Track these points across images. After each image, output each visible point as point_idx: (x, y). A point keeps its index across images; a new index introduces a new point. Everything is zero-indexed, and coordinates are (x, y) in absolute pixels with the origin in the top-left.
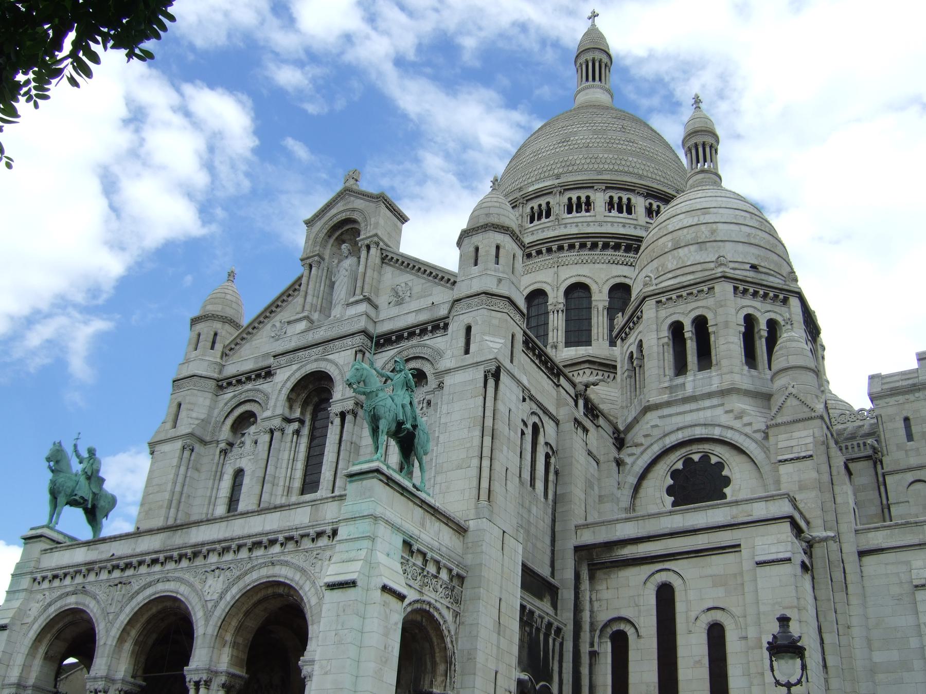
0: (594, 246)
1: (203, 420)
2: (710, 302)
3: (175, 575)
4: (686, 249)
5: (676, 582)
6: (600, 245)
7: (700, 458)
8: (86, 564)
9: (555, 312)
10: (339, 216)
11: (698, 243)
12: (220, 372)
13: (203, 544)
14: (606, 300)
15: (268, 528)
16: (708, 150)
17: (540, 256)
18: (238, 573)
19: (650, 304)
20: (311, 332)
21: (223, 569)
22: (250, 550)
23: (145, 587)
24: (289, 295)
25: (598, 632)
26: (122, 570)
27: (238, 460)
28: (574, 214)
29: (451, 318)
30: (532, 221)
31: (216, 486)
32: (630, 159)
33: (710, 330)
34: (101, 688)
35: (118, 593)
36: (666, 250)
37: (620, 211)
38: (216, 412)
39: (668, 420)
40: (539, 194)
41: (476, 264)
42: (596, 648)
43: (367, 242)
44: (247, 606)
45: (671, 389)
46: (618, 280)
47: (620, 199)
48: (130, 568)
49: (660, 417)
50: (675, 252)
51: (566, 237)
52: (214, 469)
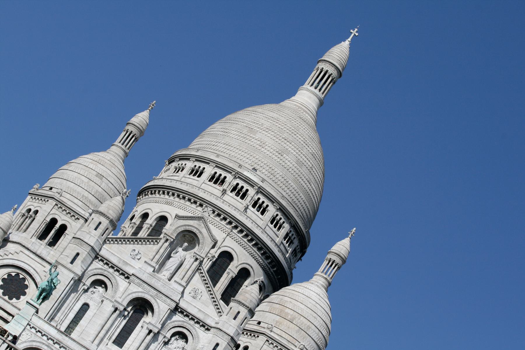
9: (209, 260)
12: (100, 250)
14: (235, 274)
17: (223, 221)
20: (154, 279)
27: (89, 300)
28: (254, 210)
29: (212, 330)
32: (301, 195)
36: (287, 318)
40: (247, 180)
41: (235, 319)
43: (198, 257)
46: (247, 267)
47: (281, 219)
51: (243, 225)
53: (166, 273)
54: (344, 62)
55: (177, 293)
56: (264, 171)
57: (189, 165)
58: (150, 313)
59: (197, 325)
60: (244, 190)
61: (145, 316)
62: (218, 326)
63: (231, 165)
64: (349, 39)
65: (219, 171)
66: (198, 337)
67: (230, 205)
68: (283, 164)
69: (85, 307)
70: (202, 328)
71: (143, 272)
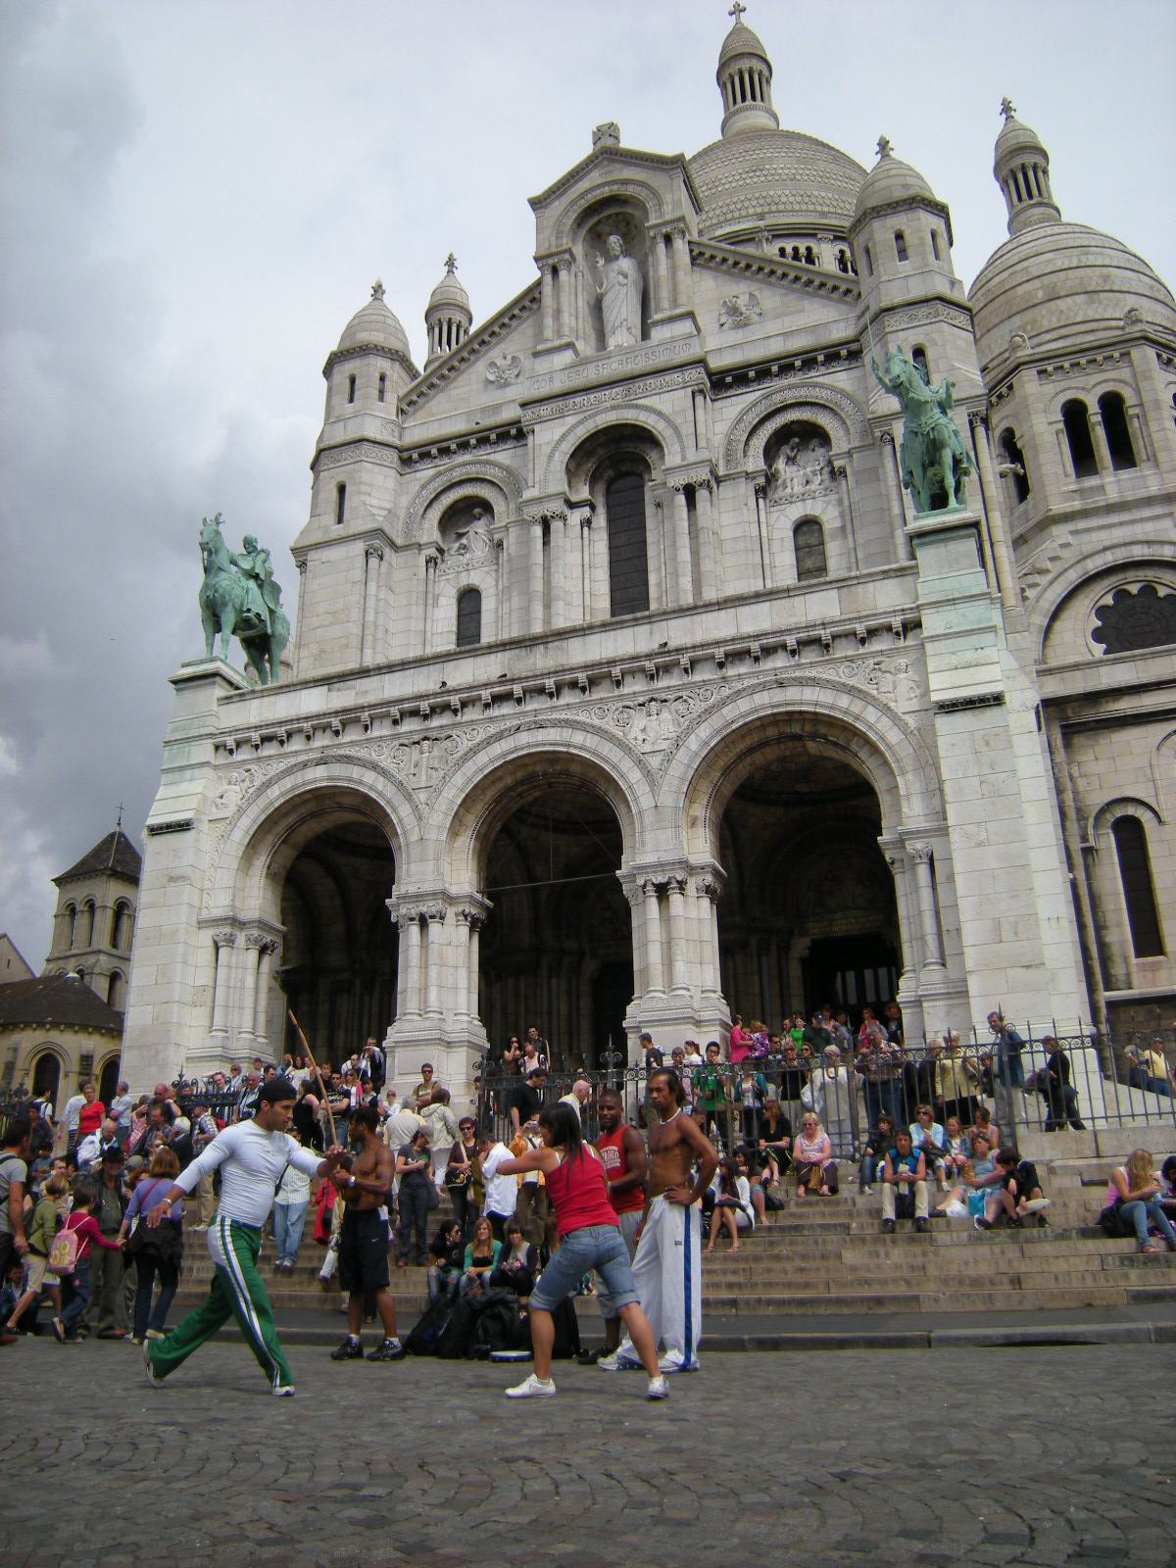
1: (390, 511)
2: (1124, 373)
3: (553, 716)
4: (1069, 299)
7: (1141, 590)
8: (337, 713)
10: (598, 191)
11: (1086, 293)
13: (612, 662)
15: (748, 629)
16: (1040, 174)
18: (704, 705)
21: (665, 701)
22: (721, 665)
23: (489, 741)
24: (513, 317)
25: (1091, 821)
26: (426, 717)
27: (463, 574)
31: (429, 615)
33: (1131, 412)
34: (434, 910)
35: (429, 754)
36: (1036, 301)
38: (404, 501)
39: (1085, 537)
41: (903, 254)
42: (1092, 843)
44: (726, 759)
45: (1081, 492)
48: (441, 713)
49: (1072, 533)
50: (1051, 304)
52: (422, 588)
53: (622, 337)
55: (682, 343)
56: (751, 211)
58: (652, 456)
59: (816, 376)
61: (647, 477)
62: (874, 309)
68: (777, 178)
69: (469, 599)
71: (547, 377)
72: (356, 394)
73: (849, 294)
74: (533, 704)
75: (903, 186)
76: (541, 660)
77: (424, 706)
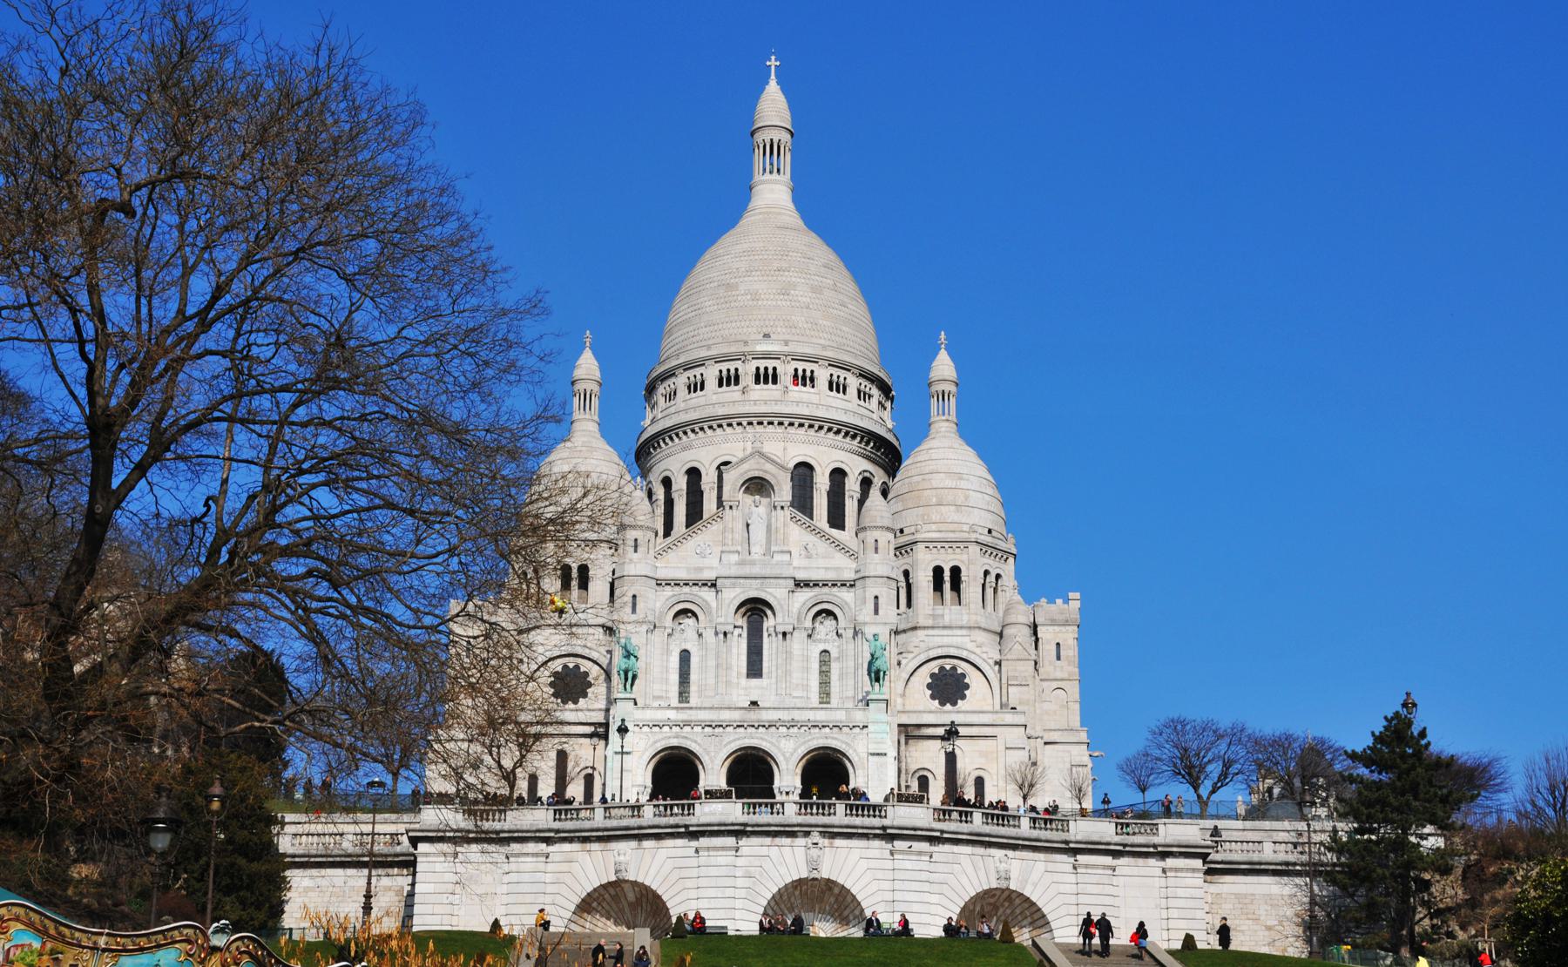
0: (821, 428)
2: (965, 557)
5: (957, 751)
6: (826, 429)
15: (818, 718)
18: (802, 740)
19: (921, 546)
23: (735, 740)
29: (857, 583)
30: (757, 381)
32: (844, 328)
37: (838, 391)
38: (658, 605)
43: (783, 504)
45: (934, 616)
47: (838, 377)
53: (758, 550)
54: (787, 115)
57: (681, 380)
58: (769, 612)
59: (835, 589)
60: (770, 371)
61: (765, 619)
63: (733, 349)
64: (773, 77)
65: (724, 367)
66: (846, 603)
67: (765, 402)
69: (685, 656)
70: (844, 588)
72: (639, 549)
73: (852, 555)
74: (751, 730)
75: (882, 517)
76: (753, 716)
77: (714, 725)
